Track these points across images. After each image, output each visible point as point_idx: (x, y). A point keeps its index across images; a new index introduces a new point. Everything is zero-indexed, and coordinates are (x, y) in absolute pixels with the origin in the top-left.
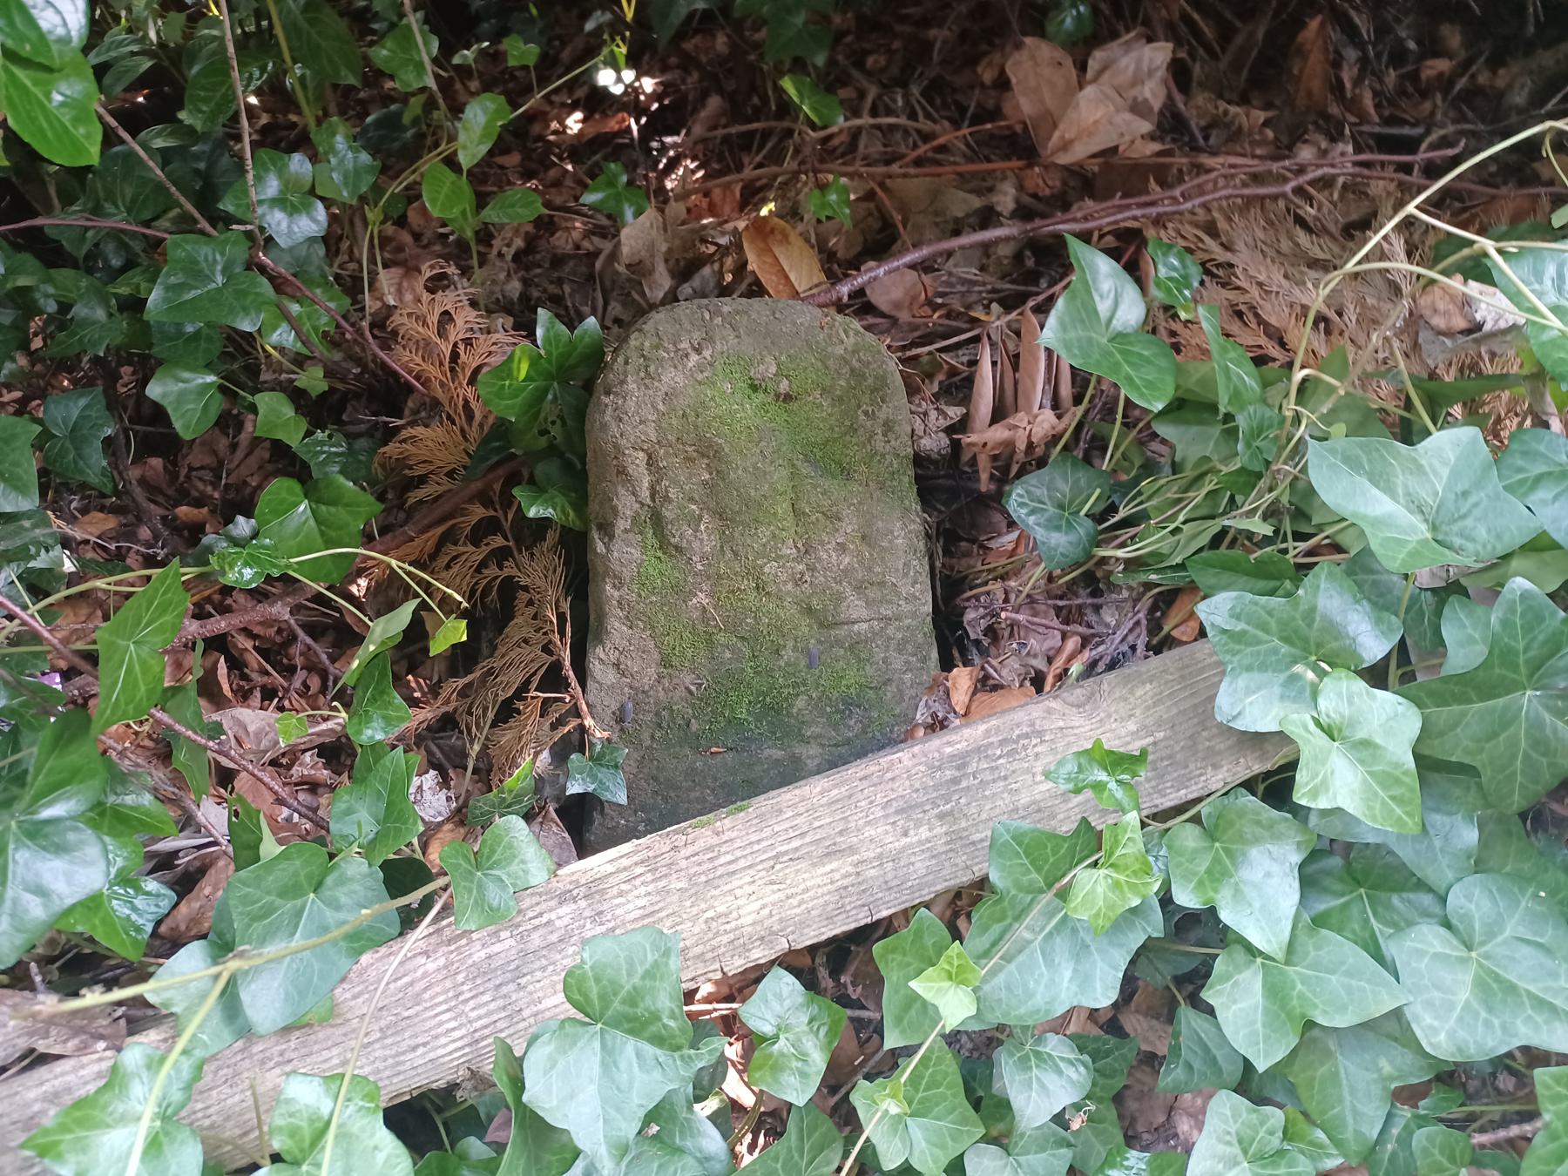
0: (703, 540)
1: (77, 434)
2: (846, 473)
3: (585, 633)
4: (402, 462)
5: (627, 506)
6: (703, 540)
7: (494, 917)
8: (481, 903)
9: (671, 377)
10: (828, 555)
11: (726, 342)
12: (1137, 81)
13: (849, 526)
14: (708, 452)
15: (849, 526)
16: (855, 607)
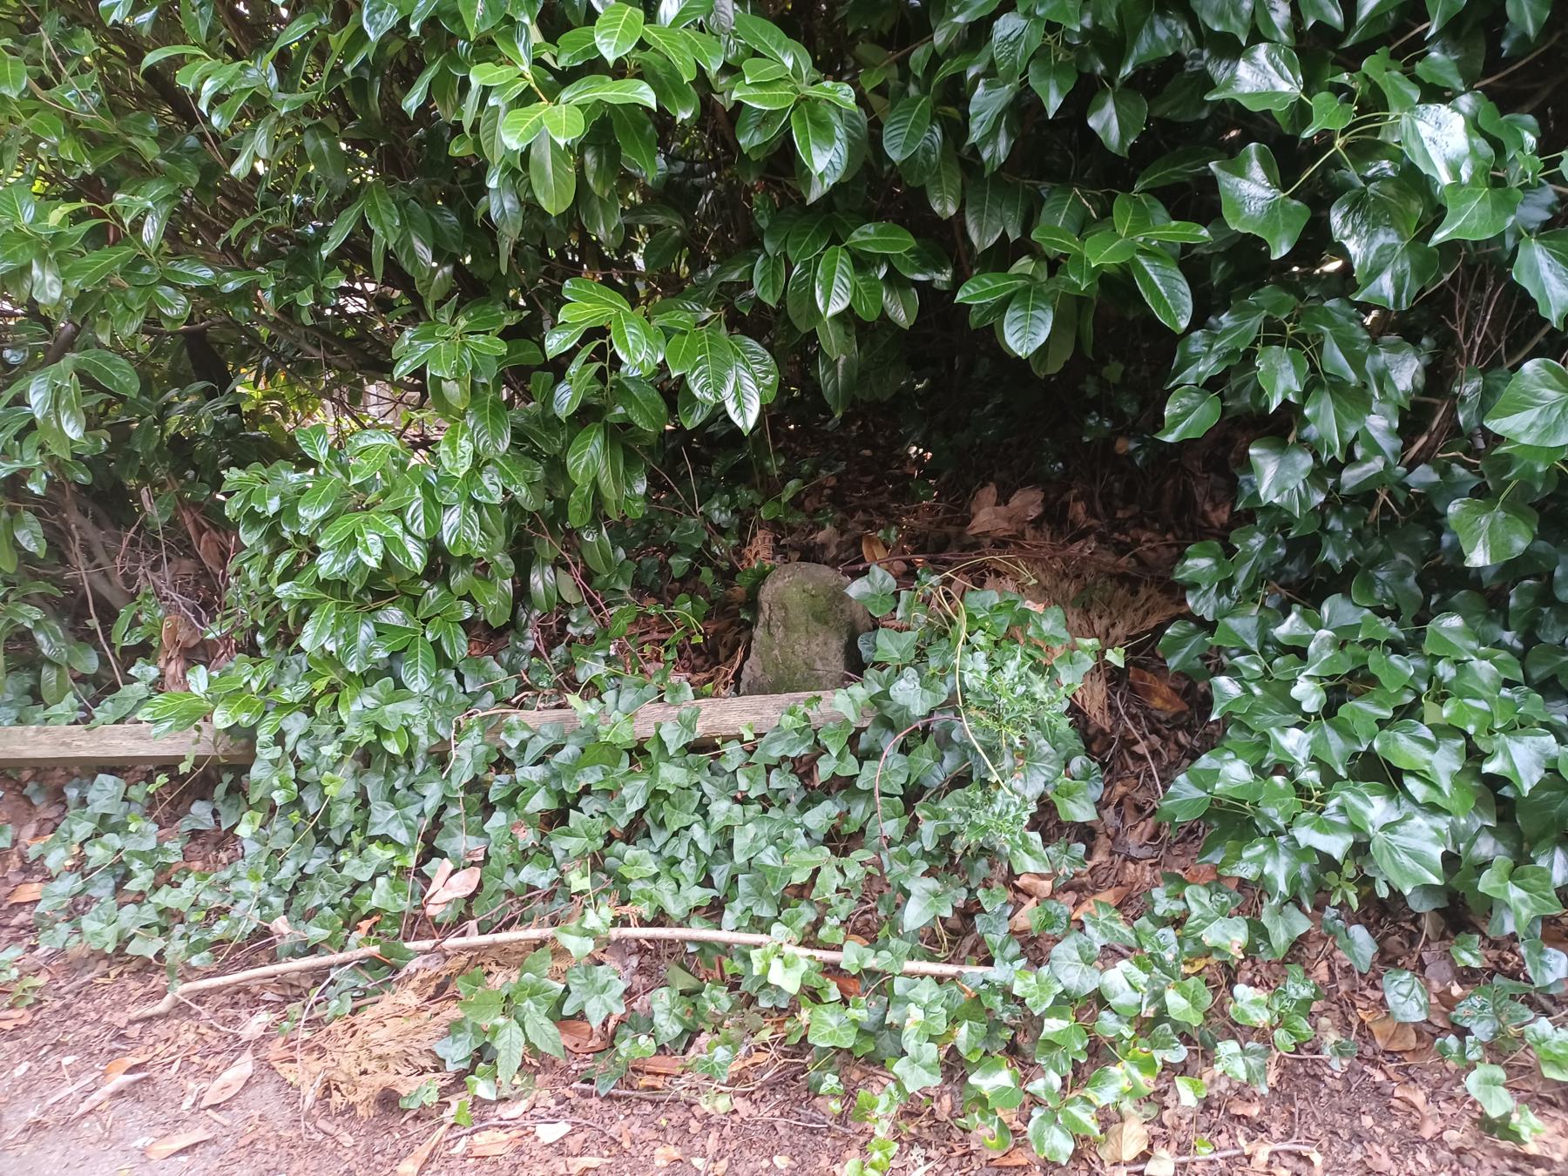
0: (779, 633)
1: (648, 570)
2: (826, 623)
3: (746, 656)
4: (729, 597)
5: (762, 619)
6: (779, 633)
7: (674, 704)
8: (673, 698)
9: (779, 584)
10: (813, 646)
11: (799, 576)
12: (1025, 506)
13: (821, 639)
14: (784, 607)
15: (821, 639)
16: (819, 665)
